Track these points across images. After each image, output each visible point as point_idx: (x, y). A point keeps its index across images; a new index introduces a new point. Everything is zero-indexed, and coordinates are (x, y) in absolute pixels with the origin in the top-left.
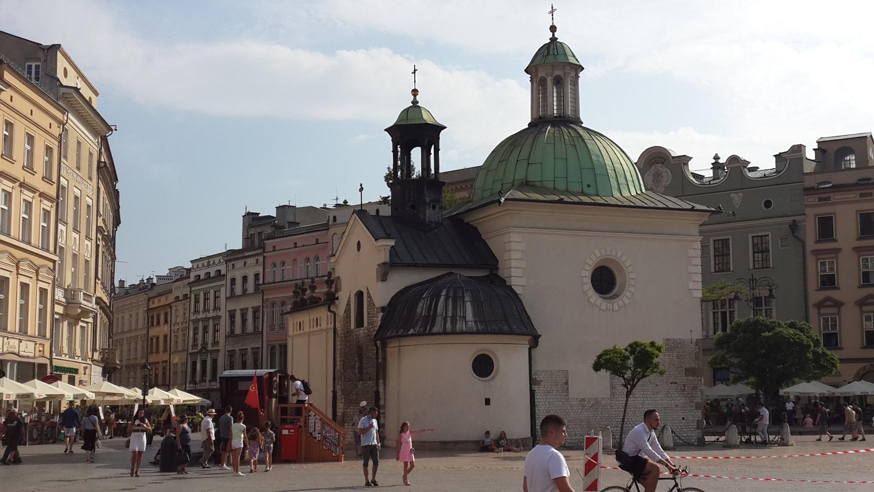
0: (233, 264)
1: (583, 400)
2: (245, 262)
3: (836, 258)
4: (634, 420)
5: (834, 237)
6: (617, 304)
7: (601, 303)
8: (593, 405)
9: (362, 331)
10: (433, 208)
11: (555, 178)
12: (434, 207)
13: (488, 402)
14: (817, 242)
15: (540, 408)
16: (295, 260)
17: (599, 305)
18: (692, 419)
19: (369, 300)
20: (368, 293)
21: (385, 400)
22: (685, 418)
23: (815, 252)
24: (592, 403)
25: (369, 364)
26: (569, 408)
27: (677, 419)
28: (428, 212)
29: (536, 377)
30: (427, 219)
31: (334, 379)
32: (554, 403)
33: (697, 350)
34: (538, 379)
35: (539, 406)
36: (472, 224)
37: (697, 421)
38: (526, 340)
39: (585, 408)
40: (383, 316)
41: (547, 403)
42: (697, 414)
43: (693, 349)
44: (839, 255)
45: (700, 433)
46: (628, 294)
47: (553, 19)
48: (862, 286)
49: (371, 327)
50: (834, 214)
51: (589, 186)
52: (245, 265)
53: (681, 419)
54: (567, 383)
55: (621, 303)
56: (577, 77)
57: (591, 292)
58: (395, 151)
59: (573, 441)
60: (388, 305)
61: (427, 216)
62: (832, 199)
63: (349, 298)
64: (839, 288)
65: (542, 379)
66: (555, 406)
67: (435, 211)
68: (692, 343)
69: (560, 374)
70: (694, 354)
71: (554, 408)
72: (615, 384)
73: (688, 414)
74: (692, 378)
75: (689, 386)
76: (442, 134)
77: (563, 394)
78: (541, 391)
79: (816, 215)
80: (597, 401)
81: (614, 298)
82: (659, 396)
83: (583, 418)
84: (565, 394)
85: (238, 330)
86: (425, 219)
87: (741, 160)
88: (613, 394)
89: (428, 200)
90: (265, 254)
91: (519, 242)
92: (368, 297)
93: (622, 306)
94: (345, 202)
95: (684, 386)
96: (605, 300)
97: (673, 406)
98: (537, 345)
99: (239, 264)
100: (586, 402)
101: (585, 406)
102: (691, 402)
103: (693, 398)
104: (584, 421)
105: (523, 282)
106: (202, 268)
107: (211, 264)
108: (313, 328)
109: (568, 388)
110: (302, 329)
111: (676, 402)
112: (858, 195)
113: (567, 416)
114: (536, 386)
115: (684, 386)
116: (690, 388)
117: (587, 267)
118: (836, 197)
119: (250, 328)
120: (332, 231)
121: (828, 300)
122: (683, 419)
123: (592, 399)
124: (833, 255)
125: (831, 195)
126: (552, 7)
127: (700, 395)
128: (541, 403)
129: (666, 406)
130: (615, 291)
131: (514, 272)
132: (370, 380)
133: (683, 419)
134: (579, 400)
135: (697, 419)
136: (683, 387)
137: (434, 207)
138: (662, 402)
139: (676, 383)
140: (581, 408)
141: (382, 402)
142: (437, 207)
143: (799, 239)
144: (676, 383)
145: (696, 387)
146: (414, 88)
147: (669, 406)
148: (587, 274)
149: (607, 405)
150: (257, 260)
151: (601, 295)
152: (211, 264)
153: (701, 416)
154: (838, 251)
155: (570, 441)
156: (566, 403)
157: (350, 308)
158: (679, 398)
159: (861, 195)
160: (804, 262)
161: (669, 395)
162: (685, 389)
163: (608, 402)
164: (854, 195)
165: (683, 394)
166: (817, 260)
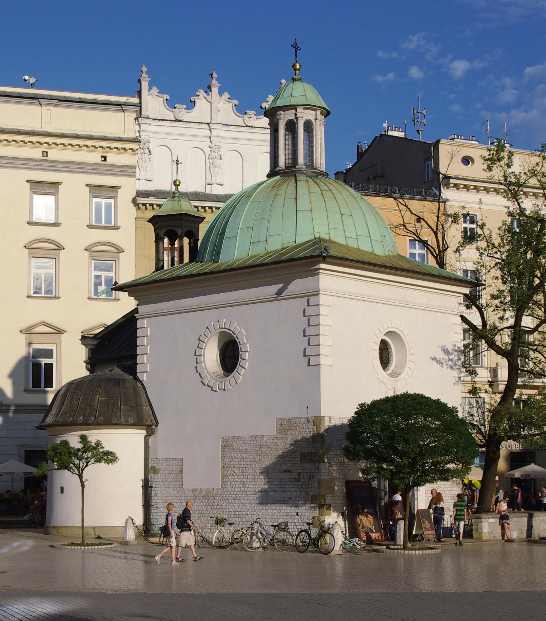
1: (195, 489)
4: (245, 513)
22: (299, 514)
34: (157, 467)
65: (161, 467)
71: (170, 498)
74: (308, 465)
75: (305, 474)
84: (180, 483)
88: (223, 483)
95: (299, 474)
102: (307, 495)
103: (308, 490)
111: (290, 493)
114: (156, 475)
116: (305, 477)
122: (297, 514)
127: (316, 486)
129: (279, 498)
133: (297, 514)
136: (297, 477)
139: (290, 471)
144: (290, 471)
145: (313, 476)
147: (281, 499)
158: (293, 489)
161: (282, 486)
162: (300, 479)
165: (298, 484)
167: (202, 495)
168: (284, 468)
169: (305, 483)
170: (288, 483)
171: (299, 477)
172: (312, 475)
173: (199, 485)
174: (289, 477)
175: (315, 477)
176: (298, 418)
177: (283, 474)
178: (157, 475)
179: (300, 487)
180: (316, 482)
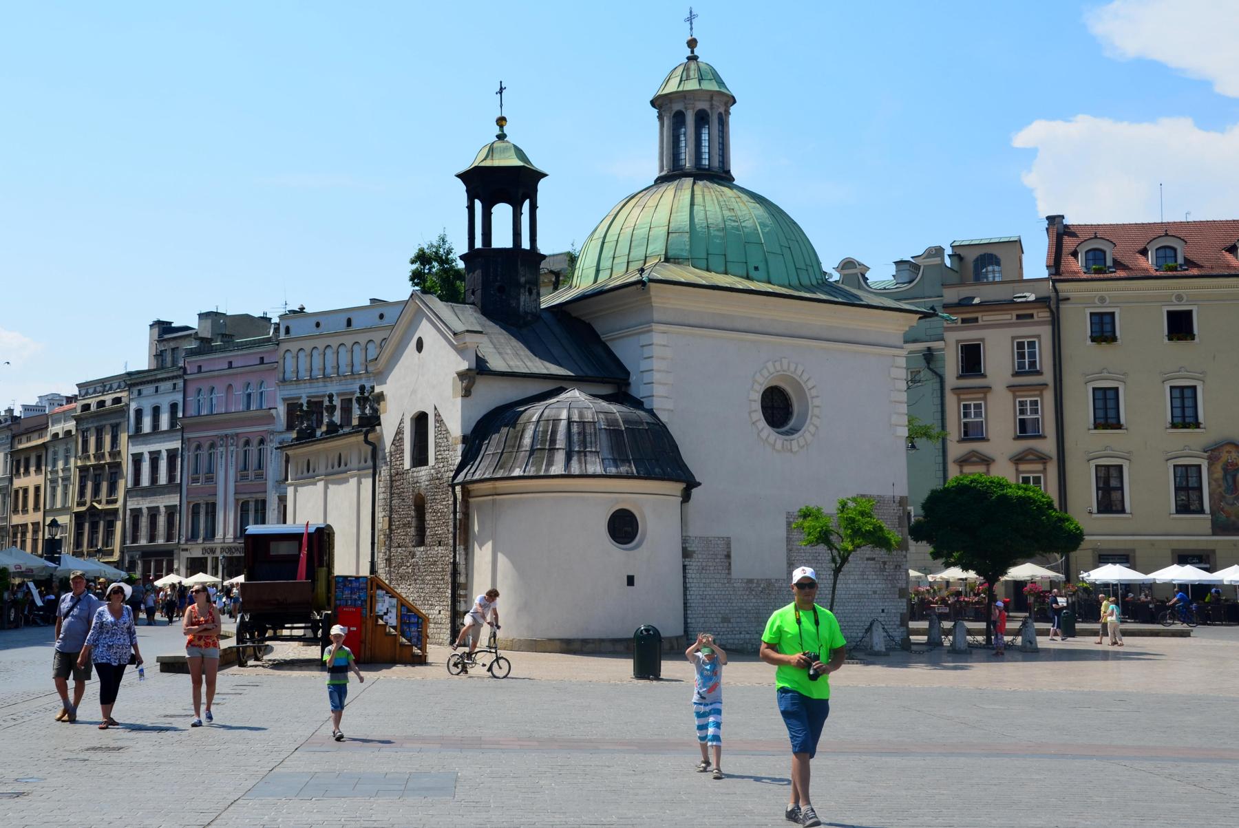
0: (139, 391)
1: (750, 581)
2: (157, 388)
3: (985, 399)
5: (982, 372)
6: (797, 440)
7: (775, 441)
8: (764, 588)
9: (423, 473)
10: (529, 291)
11: (708, 254)
12: (530, 293)
13: (631, 581)
14: (960, 377)
15: (691, 593)
16: (230, 386)
17: (772, 442)
18: (895, 611)
19: (438, 425)
20: (437, 415)
21: (467, 575)
22: (886, 611)
23: (956, 390)
24: (762, 586)
25: (436, 522)
26: (731, 593)
27: (874, 611)
28: (522, 298)
29: (687, 545)
30: (521, 309)
31: (373, 544)
32: (712, 585)
33: (901, 511)
34: (689, 549)
35: (690, 589)
36: (583, 319)
37: (901, 614)
38: (677, 488)
39: (753, 593)
40: (464, 449)
41: (702, 585)
42: (900, 604)
43: (895, 511)
44: (989, 396)
45: (904, 632)
46: (812, 429)
47: (691, 29)
48: (1017, 438)
49: (441, 465)
50: (983, 340)
51: (756, 268)
52: (157, 391)
53: (881, 611)
54: (728, 556)
55: (802, 442)
56: (727, 113)
57: (763, 423)
58: (471, 209)
59: (736, 642)
60: (472, 432)
61: (522, 303)
62: (980, 319)
63: (402, 422)
64: (988, 440)
65: (695, 549)
66: (713, 589)
67: (532, 297)
68: (894, 502)
69: (719, 542)
70: (897, 518)
71: (710, 593)
72: (793, 558)
73: (890, 604)
75: (891, 563)
76: (542, 185)
77: (723, 572)
78: (693, 567)
79: (958, 342)
80: (769, 583)
81: (793, 434)
82: (852, 577)
83: (750, 608)
84: (727, 571)
85: (145, 481)
86: (519, 307)
87: (859, 265)
89: (523, 280)
90: (186, 377)
91: (664, 346)
92: (436, 421)
93: (804, 446)
94: (302, 309)
95: (885, 563)
96: (780, 436)
97: (870, 593)
98: (690, 499)
99: (148, 390)
100: (755, 585)
101: (753, 590)
103: (895, 581)
104: (752, 611)
105: (669, 405)
106: (94, 395)
107: (107, 388)
108: (333, 468)
109: (730, 564)
110: (342, 464)
111: (874, 586)
112: (1015, 317)
113: (729, 604)
114: (687, 560)
115: (885, 563)
116: (892, 567)
117: (757, 387)
118: (985, 318)
119: (163, 479)
120: (284, 347)
121: (974, 456)
122: (883, 611)
123: (762, 580)
124: (981, 395)
125: (979, 315)
126: (691, 12)
128: (693, 585)
129: (861, 592)
130: (792, 423)
131: (658, 390)
132: (440, 545)
133: (883, 611)
134: (745, 581)
135: (901, 611)
136: (882, 565)
137: (530, 293)
138: (855, 586)
139: (873, 559)
140: (747, 593)
141: (462, 579)
142: (534, 291)
143: (936, 373)
144: (873, 559)
145: (900, 566)
146: (500, 115)
147: (864, 593)
148: (757, 397)
149: (783, 589)
150: (175, 385)
151: (775, 429)
152: (107, 388)
153: (906, 607)
154: (987, 389)
155: (731, 641)
156: (727, 585)
157: (402, 439)
158: (877, 582)
159: (1019, 317)
160: (943, 405)
161: (865, 577)
162: (885, 569)
163: (784, 585)
164: (1009, 317)
166: (959, 401)
167: (760, 589)
168: (867, 556)
169: (891, 573)
170: (873, 573)
171: (884, 566)
172: (899, 564)
173: (756, 575)
174: (874, 566)
175: (902, 567)
176: (881, 497)
177: (866, 562)
178: (689, 560)
179: (885, 578)
180: (904, 573)
